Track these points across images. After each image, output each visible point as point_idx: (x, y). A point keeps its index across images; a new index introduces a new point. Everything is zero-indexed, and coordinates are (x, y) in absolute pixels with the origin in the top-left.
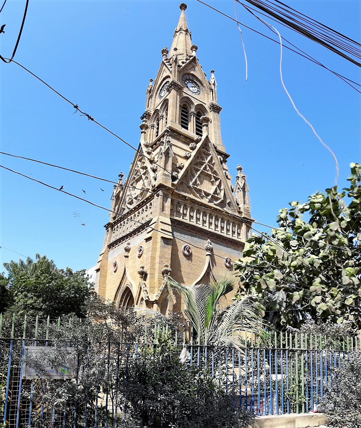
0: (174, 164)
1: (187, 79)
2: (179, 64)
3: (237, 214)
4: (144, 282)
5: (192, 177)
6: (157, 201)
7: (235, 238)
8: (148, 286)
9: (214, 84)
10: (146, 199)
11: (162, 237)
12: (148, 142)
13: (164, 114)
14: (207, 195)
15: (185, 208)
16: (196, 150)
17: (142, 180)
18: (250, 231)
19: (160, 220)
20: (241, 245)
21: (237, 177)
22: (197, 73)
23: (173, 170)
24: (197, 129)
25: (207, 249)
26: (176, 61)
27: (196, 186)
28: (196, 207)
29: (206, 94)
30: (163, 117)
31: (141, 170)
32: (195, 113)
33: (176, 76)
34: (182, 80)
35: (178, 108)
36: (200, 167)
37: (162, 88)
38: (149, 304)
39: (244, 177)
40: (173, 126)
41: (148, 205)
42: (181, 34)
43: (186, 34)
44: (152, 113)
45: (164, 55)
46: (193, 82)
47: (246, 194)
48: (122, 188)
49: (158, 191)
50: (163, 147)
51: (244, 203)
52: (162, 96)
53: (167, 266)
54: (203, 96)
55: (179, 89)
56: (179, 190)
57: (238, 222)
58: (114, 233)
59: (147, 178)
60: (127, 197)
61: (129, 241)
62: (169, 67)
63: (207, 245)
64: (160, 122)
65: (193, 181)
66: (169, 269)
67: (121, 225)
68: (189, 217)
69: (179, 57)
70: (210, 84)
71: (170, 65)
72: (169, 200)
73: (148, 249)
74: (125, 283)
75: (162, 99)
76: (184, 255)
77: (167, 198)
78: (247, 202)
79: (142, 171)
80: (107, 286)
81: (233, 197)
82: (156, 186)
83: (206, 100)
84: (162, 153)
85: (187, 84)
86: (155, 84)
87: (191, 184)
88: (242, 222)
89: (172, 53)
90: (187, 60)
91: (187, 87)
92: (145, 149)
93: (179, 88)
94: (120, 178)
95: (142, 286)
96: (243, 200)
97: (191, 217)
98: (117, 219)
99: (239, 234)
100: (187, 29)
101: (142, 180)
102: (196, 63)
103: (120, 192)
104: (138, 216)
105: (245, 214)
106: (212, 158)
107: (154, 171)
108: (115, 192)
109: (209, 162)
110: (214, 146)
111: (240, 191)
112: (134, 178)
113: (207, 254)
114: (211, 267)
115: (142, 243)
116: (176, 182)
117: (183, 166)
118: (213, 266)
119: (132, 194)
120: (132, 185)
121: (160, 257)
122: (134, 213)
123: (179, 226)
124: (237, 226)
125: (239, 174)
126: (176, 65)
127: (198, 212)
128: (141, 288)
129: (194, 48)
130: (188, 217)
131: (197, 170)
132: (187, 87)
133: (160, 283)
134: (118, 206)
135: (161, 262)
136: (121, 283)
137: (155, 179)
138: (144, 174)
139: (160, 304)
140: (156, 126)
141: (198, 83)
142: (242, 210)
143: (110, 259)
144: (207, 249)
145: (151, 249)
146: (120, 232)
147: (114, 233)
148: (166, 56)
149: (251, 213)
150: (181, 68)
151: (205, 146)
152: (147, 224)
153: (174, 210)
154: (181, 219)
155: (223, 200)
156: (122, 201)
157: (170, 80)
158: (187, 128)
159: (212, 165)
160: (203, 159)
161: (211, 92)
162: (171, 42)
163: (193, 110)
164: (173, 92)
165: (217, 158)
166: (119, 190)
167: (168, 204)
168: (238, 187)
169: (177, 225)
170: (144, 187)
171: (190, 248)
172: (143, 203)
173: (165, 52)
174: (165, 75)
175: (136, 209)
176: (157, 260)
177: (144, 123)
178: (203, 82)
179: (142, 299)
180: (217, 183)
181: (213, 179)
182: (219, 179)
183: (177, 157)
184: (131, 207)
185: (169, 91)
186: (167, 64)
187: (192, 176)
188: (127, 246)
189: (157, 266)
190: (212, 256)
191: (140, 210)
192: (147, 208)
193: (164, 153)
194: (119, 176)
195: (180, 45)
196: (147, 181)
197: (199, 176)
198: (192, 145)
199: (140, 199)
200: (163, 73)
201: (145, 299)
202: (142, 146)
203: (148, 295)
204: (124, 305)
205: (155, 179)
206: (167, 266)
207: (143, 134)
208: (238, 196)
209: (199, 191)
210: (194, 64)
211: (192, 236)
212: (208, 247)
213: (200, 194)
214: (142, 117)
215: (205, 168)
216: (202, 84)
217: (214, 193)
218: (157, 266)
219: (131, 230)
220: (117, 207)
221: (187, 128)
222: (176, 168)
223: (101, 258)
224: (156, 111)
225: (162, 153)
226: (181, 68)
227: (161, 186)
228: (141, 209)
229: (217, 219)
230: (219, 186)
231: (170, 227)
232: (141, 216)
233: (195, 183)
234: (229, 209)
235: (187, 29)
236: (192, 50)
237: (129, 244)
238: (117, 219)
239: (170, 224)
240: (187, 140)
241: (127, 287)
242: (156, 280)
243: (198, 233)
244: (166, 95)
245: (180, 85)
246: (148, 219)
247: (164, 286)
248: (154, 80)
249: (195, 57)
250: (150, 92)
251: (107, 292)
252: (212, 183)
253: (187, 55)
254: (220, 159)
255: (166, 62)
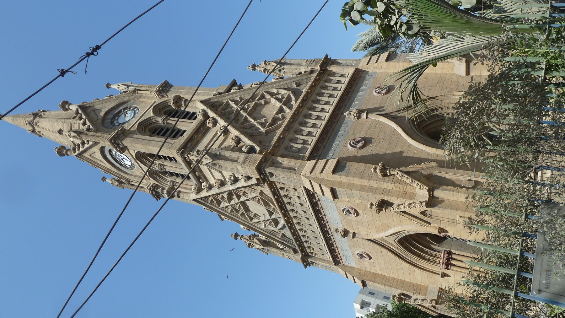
0: (233, 150)
1: (112, 123)
2: (85, 130)
3: (314, 76)
4: (395, 206)
5: (254, 129)
6: (280, 177)
7: (345, 81)
8: (402, 201)
9: (128, 86)
10: (274, 197)
11: (334, 172)
12: (193, 187)
13: (157, 162)
14: (281, 110)
15: (295, 140)
16: (219, 119)
17: (247, 202)
18: (339, 61)
19: (308, 174)
20: (358, 74)
21: (264, 72)
22: (104, 109)
23: (240, 150)
24: (189, 118)
25: (359, 117)
26: (79, 133)
27: (267, 124)
28: (296, 126)
29: (141, 100)
30: (161, 164)
31: (232, 202)
32: (164, 117)
33: (102, 135)
34: (111, 128)
35: (152, 138)
36: (242, 116)
37: (119, 163)
38: (432, 202)
39: (265, 61)
40: (177, 148)
41: (282, 193)
42: (38, 124)
43: (41, 116)
44: (152, 181)
45: (66, 152)
46: (118, 114)
47: (288, 62)
48: (255, 236)
49: (266, 174)
50: (205, 161)
51: (300, 65)
52: (130, 164)
53: (376, 169)
54: (143, 104)
55: (124, 134)
56: (269, 146)
57: (326, 76)
58: (316, 254)
59: (245, 193)
60: (268, 228)
61: (333, 230)
62: (86, 146)
63: (352, 116)
64: (169, 169)
65: (261, 128)
66: (380, 165)
67: (306, 242)
68: (310, 137)
69: (75, 128)
70: (127, 91)
71: (83, 143)
72: (280, 159)
73: (349, 196)
74: (392, 245)
75: (136, 164)
76: (363, 147)
77: (278, 162)
78: (299, 62)
79: (235, 200)
80: (391, 276)
81: (290, 78)
82: (258, 177)
83: (149, 101)
84: (213, 164)
85: (120, 124)
86: (111, 173)
87: (263, 130)
88: (327, 70)
89: (67, 141)
90: (81, 118)
91: (124, 123)
92: (204, 194)
93: (123, 133)
94: (239, 238)
95: (401, 210)
96: (295, 67)
97: (310, 134)
98: (297, 248)
99: (342, 76)
100: (33, 114)
101: (247, 202)
102: (90, 107)
103: (259, 240)
104: (297, 212)
105: (316, 65)
106: (232, 101)
107: (236, 180)
108: (257, 246)
109: (237, 104)
110: (216, 95)
111: (283, 69)
112: (243, 214)
113: (365, 118)
114: (384, 112)
115: (338, 208)
116: (258, 149)
117: (236, 137)
118: (384, 110)
119: (263, 219)
120: (251, 219)
121: (362, 177)
122: (291, 219)
123: (320, 151)
124: (331, 78)
125: (260, 69)
126: (85, 134)
127: (304, 124)
128: (404, 212)
129: (65, 105)
130: (309, 139)
131: (246, 120)
132: (124, 123)
133: (400, 182)
134: (277, 244)
135: (370, 178)
136: (390, 250)
137: (249, 178)
138: (239, 197)
139: (435, 186)
140: (174, 178)
141: (121, 108)
142: (309, 69)
143: (354, 265)
144: (359, 117)
145: (349, 190)
146: (317, 244)
147: (316, 254)
148: (69, 150)
149: (316, 58)
150: (91, 127)
151: (215, 108)
152: (311, 196)
153: (297, 155)
154: (310, 148)
155: (292, 92)
156: (271, 236)
157: (108, 146)
158: (185, 131)
159: (241, 101)
160: (231, 112)
161: (139, 92)
162: (49, 141)
163: (160, 120)
164: (126, 142)
165: (234, 93)
166: (255, 240)
167: (285, 162)
168: (278, 72)
169: (319, 152)
170: (257, 199)
171: (354, 139)
172: (278, 201)
173: (62, 151)
174: (98, 155)
175: (285, 214)
176: (365, 182)
177: (165, 192)
178: (121, 101)
179: (423, 213)
180: (268, 96)
181: (263, 102)
182: (263, 94)
183: (223, 146)
184: (282, 222)
185: (123, 149)
186: (81, 149)
187: (252, 128)
188: (339, 233)
189: (373, 184)
190: (369, 111)
191: (289, 207)
192: (286, 196)
193: (213, 161)
194: (236, 239)
195: (55, 128)
196: (249, 194)
197: (255, 119)
198: (209, 124)
199: (273, 206)
200: (95, 158)
201: (424, 208)
202: (199, 196)
203: (418, 202)
204: (426, 253)
205: (249, 178)
206: (375, 169)
207: (181, 195)
208: (289, 72)
209: (275, 120)
210: (89, 110)
211: (336, 135)
212: (355, 115)
213: (279, 119)
214: (156, 199)
215: (245, 110)
216: (124, 103)
217: (281, 102)
218: (373, 184)
219: (315, 224)
220: (279, 246)
221: (185, 131)
222: (238, 146)
223: (350, 277)
224: (152, 174)
225: (213, 164)
226: (91, 127)
227: (260, 169)
228: (287, 206)
229: (318, 102)
230: (272, 94)
231: (320, 161)
232: (298, 207)
233: (263, 125)
234: (305, 86)
235: (33, 114)
236: (67, 110)
237: (337, 230)
238: (297, 248)
239: (314, 161)
240: (202, 130)
241: (398, 241)
242: (394, 188)
243: (333, 127)
244: (130, 157)
245: (118, 131)
246: (304, 197)
247: (406, 176)
248: (102, 173)
249: (79, 106)
250: (121, 183)
251: (402, 278)
252: (267, 102)
253: (74, 118)
254: (236, 89)
255: (79, 150)
